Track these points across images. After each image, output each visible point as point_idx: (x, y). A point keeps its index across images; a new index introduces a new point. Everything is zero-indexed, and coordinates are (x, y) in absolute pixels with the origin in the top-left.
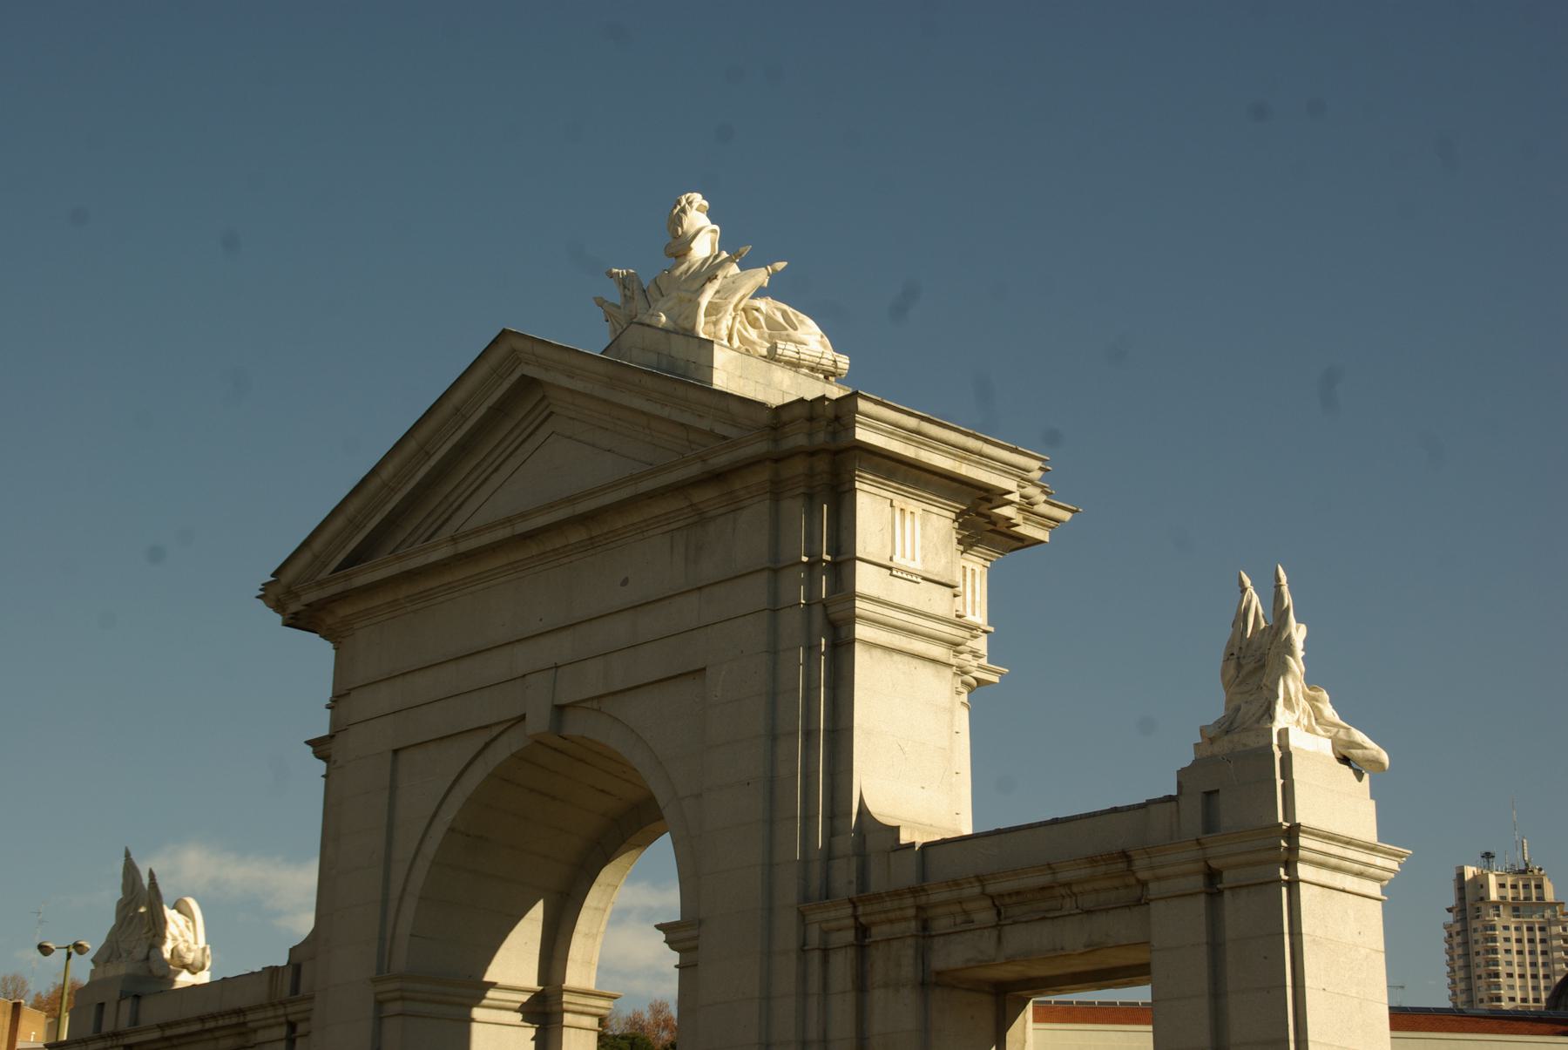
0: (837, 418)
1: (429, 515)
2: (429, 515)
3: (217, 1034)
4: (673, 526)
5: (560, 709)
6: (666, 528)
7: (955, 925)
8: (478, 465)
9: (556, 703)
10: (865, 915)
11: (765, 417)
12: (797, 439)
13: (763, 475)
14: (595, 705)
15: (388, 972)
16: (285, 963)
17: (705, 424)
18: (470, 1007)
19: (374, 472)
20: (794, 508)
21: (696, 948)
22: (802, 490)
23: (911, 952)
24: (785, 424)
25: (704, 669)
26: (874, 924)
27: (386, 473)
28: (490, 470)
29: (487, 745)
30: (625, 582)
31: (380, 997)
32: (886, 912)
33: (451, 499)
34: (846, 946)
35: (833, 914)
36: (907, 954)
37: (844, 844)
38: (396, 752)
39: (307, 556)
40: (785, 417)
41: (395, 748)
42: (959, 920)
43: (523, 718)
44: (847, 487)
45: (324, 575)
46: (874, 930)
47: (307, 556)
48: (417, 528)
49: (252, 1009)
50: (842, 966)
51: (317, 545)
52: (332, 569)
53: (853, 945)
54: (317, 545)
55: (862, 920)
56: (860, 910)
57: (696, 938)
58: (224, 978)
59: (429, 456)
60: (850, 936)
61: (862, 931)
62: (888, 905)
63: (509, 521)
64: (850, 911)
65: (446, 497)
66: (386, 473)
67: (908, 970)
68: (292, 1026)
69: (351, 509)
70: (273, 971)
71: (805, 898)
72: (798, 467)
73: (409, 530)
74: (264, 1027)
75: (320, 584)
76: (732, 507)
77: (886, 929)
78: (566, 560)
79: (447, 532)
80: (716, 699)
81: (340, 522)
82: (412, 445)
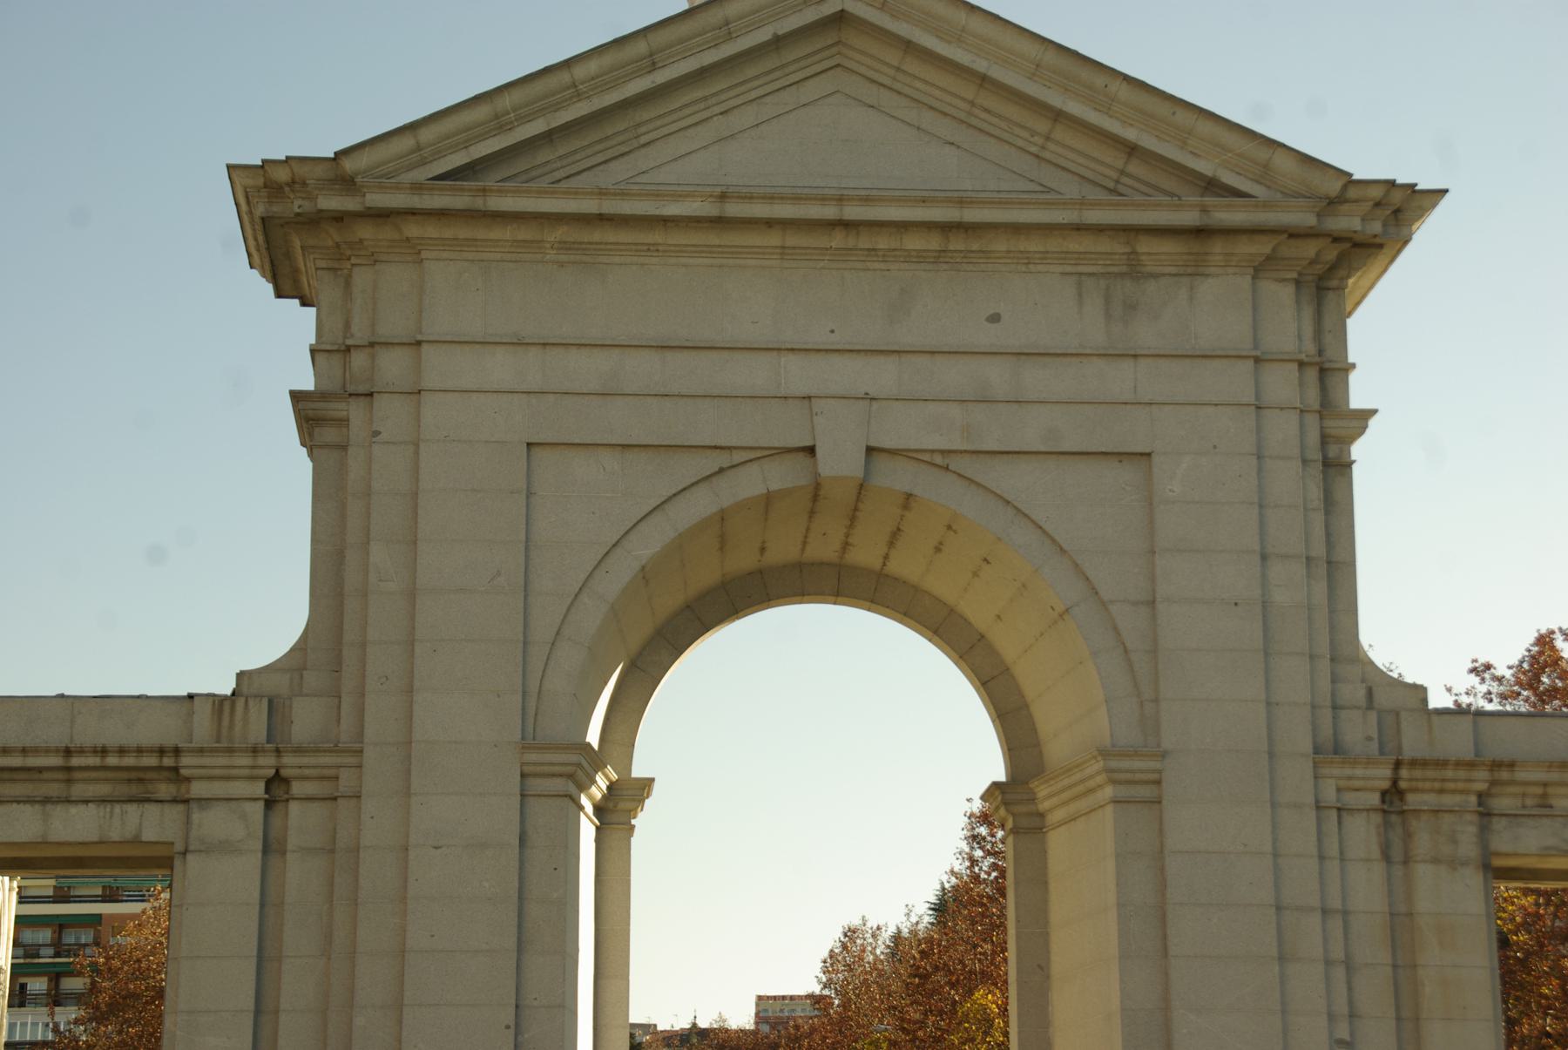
0: (1397, 212)
1: (600, 141)
2: (600, 141)
3: (77, 775)
4: (1081, 269)
5: (870, 450)
6: (1069, 269)
7: (1524, 807)
8: (705, 98)
9: (869, 444)
10: (1411, 780)
11: (1334, 188)
12: (1348, 222)
13: (1263, 247)
14: (938, 459)
15: (534, 739)
16: (229, 692)
17: (1204, 167)
18: (581, 792)
19: (567, 64)
20: (1280, 295)
21: (1158, 782)
22: (1295, 275)
23: (1472, 829)
24: (1346, 201)
25: (1149, 455)
26: (1415, 790)
27: (580, 72)
28: (717, 110)
29: (721, 470)
30: (995, 318)
31: (527, 769)
32: (1443, 780)
33: (643, 129)
34: (1368, 810)
35: (1359, 772)
36: (1468, 832)
37: (1353, 693)
38: (529, 445)
39: (407, 142)
40: (1352, 193)
41: (529, 441)
42: (1529, 802)
43: (811, 450)
44: (1334, 283)
45: (421, 175)
46: (1410, 797)
47: (407, 142)
48: (575, 152)
49: (201, 751)
50: (1362, 833)
51: (426, 135)
52: (441, 171)
53: (1375, 810)
54: (426, 135)
55: (1403, 785)
56: (1404, 773)
57: (1160, 772)
58: (62, 696)
59: (653, 67)
60: (1375, 799)
61: (1393, 794)
62: (1450, 773)
63: (840, 200)
64: (1387, 772)
65: (639, 125)
66: (580, 72)
67: (1468, 846)
68: (277, 782)
69: (506, 101)
70: (217, 702)
71: (1317, 750)
72: (1309, 249)
73: (561, 151)
74: (201, 778)
75: (417, 188)
76: (1190, 270)
77: (1430, 799)
78: (882, 266)
79: (618, 172)
80: (1171, 493)
81: (482, 112)
82: (641, 47)
